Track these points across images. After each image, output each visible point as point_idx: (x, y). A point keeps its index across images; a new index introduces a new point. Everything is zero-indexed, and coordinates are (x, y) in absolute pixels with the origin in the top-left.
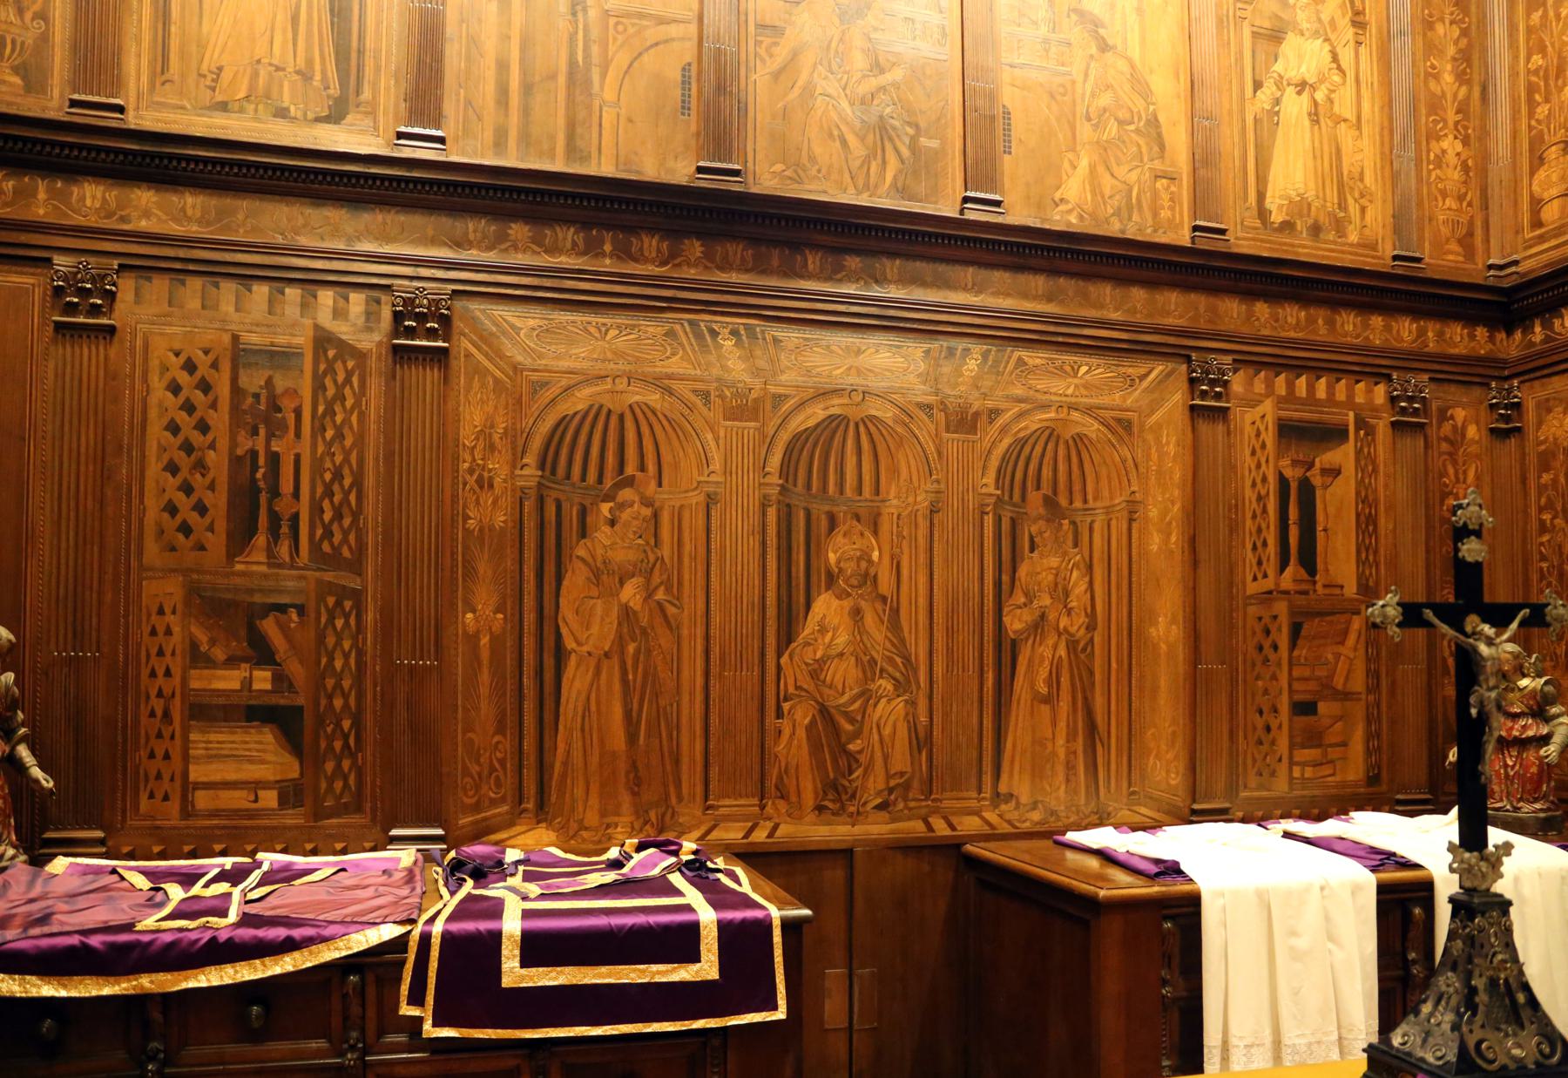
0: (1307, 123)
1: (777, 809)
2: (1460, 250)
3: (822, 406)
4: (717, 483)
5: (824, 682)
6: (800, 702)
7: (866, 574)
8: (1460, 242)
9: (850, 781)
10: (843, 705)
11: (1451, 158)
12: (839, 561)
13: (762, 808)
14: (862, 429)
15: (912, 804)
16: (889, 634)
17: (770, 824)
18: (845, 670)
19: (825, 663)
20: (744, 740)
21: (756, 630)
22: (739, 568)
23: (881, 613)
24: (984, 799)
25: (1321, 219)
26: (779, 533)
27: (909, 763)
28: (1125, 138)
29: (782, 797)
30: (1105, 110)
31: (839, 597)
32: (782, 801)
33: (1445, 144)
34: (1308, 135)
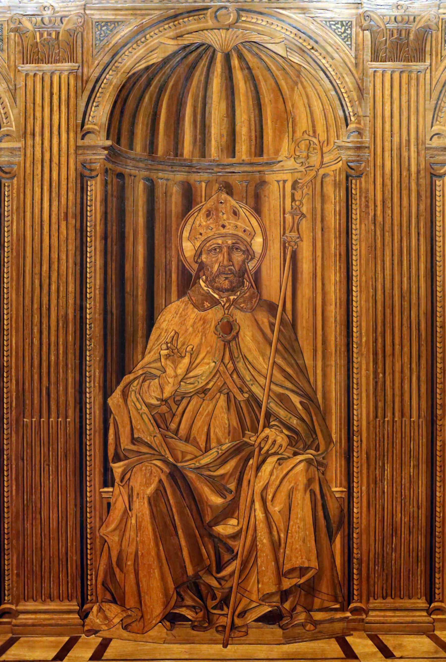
1: (106, 618)
3: (172, 34)
4: (12, 150)
5: (177, 432)
6: (140, 462)
10: (207, 466)
13: (84, 615)
14: (235, 62)
15: (318, 616)
16: (280, 361)
18: (211, 415)
20: (54, 516)
21: (70, 356)
22: (45, 267)
23: (268, 331)
26: (105, 214)
27: (314, 557)
29: (114, 601)
31: (199, 306)
32: (113, 606)
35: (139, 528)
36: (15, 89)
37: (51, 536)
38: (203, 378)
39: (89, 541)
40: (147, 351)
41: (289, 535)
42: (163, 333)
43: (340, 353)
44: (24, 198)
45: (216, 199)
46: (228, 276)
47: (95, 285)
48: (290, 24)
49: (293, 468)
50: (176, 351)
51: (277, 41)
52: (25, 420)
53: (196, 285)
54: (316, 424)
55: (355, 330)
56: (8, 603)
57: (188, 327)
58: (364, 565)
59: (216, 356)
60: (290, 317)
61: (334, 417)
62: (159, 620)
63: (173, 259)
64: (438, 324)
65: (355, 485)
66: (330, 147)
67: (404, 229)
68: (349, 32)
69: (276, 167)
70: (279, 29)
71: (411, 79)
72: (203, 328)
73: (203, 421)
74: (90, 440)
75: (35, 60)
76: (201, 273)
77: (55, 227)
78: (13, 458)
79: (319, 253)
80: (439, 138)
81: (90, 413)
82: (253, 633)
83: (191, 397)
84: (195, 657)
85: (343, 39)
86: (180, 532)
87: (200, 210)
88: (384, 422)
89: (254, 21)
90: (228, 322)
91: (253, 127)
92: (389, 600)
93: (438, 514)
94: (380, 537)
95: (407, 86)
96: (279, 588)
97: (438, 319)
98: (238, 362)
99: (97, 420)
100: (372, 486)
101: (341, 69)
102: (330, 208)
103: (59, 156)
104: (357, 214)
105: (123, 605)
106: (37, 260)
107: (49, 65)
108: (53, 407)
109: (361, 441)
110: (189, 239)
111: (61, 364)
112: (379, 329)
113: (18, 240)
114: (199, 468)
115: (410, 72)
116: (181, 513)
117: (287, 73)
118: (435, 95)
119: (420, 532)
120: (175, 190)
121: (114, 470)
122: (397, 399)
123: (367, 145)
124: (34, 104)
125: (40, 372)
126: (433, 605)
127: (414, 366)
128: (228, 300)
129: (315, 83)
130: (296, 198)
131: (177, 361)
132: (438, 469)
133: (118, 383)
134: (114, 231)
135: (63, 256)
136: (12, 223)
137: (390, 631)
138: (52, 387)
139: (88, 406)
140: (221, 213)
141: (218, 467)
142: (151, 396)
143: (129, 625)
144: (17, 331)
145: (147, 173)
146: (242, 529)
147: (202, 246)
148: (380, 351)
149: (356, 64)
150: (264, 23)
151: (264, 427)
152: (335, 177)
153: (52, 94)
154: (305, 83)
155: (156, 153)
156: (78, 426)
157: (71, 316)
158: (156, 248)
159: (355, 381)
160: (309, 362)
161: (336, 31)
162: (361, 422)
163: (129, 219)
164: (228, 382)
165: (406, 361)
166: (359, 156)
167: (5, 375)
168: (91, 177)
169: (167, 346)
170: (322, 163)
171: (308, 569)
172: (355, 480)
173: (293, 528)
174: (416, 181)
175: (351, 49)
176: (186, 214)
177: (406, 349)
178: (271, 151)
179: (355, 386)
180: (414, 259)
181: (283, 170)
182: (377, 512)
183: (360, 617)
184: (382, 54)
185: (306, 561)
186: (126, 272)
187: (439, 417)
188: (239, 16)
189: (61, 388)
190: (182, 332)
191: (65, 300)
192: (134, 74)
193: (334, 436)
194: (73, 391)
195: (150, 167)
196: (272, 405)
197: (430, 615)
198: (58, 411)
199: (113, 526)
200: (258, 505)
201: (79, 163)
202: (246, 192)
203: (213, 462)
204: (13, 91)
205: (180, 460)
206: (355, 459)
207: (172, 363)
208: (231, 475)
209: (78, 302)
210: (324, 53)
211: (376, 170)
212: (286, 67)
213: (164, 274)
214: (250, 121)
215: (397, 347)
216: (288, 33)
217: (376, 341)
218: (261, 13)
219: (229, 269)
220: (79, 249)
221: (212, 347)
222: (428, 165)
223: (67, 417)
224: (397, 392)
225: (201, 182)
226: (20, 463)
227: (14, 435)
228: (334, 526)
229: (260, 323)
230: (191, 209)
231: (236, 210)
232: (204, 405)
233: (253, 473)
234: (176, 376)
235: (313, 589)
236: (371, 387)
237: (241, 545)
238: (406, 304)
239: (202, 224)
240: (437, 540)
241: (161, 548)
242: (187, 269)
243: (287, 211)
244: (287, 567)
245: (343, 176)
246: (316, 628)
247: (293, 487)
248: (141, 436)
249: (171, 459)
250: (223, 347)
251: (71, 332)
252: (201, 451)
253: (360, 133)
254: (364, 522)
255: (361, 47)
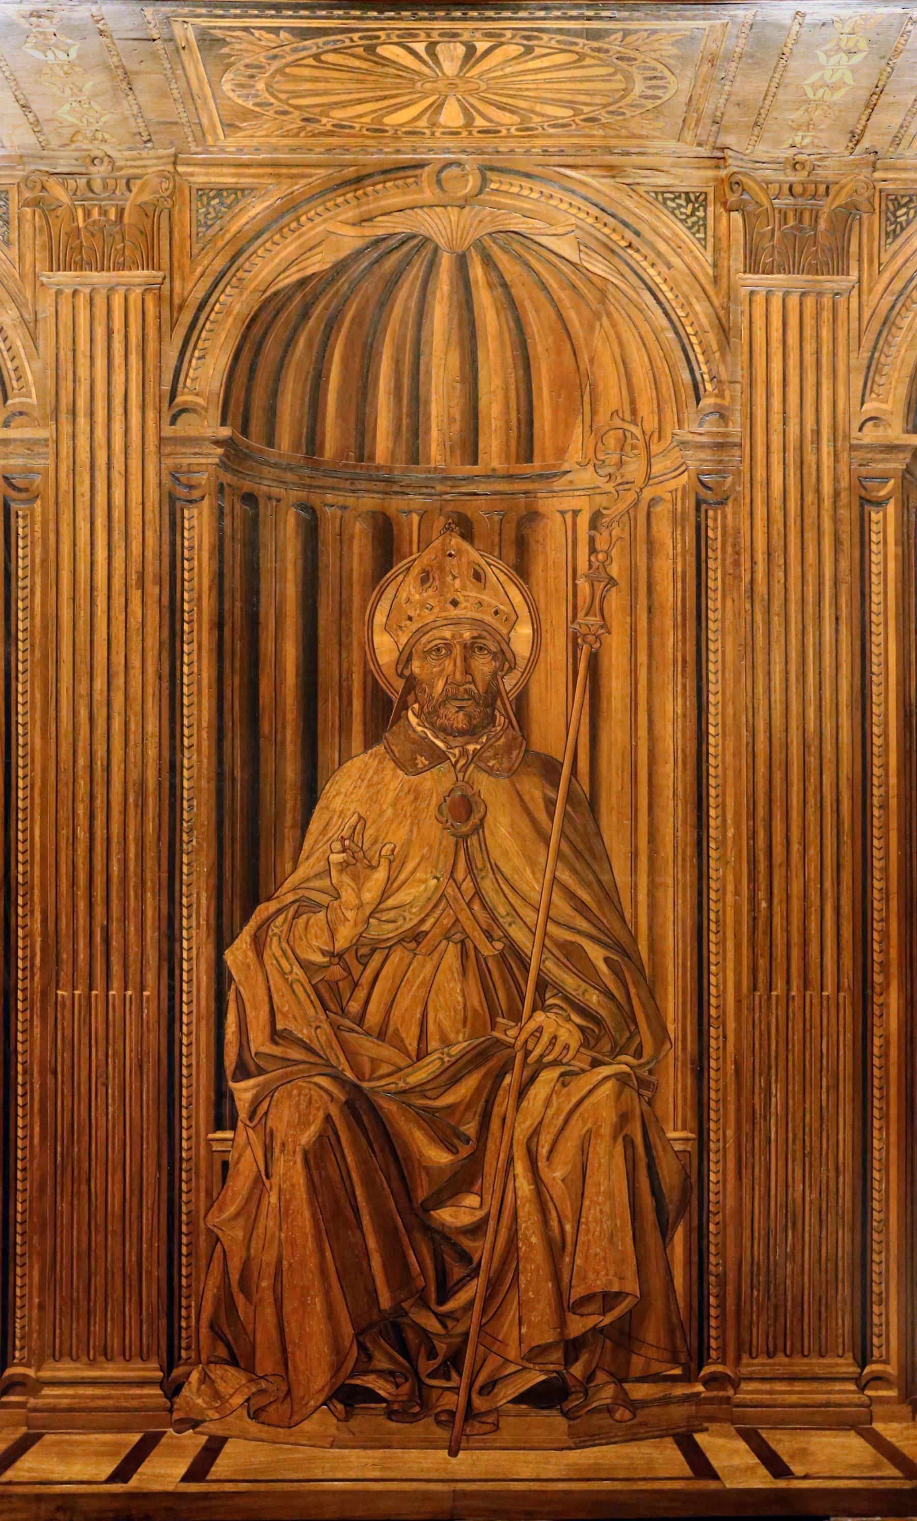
1: (217, 1395)
4: (30, 444)
5: (361, 1019)
7: (492, 695)
9: (442, 1318)
10: (421, 1089)
12: (405, 658)
13: (173, 1390)
14: (477, 272)
15: (640, 1391)
16: (565, 876)
17: (194, 1441)
18: (429, 985)
19: (363, 962)
20: (115, 1189)
21: (150, 863)
22: (100, 683)
24: (879, 1379)
27: (630, 1270)
29: (233, 1361)
31: (406, 765)
32: (231, 1371)
35: (284, 1213)
36: (36, 321)
37: (110, 1228)
38: (414, 910)
39: (184, 1240)
40: (303, 854)
41: (583, 1227)
42: (336, 817)
43: (683, 860)
44: (57, 542)
45: (440, 546)
46: (464, 704)
47: (199, 721)
48: (585, 199)
49: (590, 1092)
50: (361, 855)
51: (561, 230)
52: (60, 992)
53: (402, 722)
54: (635, 1002)
55: (712, 812)
56: (21, 1364)
57: (384, 807)
58: (730, 1289)
59: (440, 866)
60: (586, 788)
61: (671, 989)
62: (321, 1399)
63: (355, 669)
64: (876, 801)
65: (712, 1125)
66: (665, 444)
67: (810, 609)
68: (701, 213)
69: (559, 484)
70: (564, 206)
71: (822, 309)
72: (415, 809)
73: (414, 997)
74: (189, 1034)
75: (76, 263)
76: (410, 698)
77: (118, 601)
78: (36, 1069)
79: (643, 658)
80: (875, 425)
81: (190, 981)
82: (510, 1427)
83: (390, 947)
84: (393, 1475)
85: (689, 228)
86: (366, 1220)
87: (408, 569)
88: (769, 998)
89: (515, 190)
90: (463, 797)
91: (513, 403)
92: (781, 1358)
93: (876, 1185)
94: (762, 1232)
95: (813, 322)
96: (561, 1334)
97: (876, 791)
98: (482, 878)
99: (203, 994)
100: (746, 1128)
101: (685, 288)
102: (665, 566)
103: (126, 458)
104: (716, 579)
105: (250, 1369)
106: (83, 668)
107: (104, 274)
108: (116, 968)
109: (725, 1037)
110: (386, 628)
111: (132, 881)
112: (761, 812)
113: (45, 627)
114: (404, 1092)
115: (820, 294)
116: (369, 1182)
117: (582, 297)
118: (868, 340)
119: (840, 1221)
120: (359, 528)
121: (236, 1095)
122: (795, 953)
123: (737, 440)
124: (74, 351)
125: (91, 896)
126: (867, 1369)
127: (828, 884)
128: (464, 753)
129: (635, 313)
130: (598, 547)
131: (362, 876)
132: (876, 1093)
133: (245, 919)
134: (237, 611)
135: (136, 662)
136: (33, 592)
137: (783, 1422)
138: (114, 926)
139: (185, 966)
140: (451, 577)
141: (442, 1090)
142: (311, 946)
143: (262, 1409)
144: (44, 812)
145: (301, 494)
146: (488, 1215)
147: (412, 641)
148: (761, 857)
149: (715, 277)
150: (535, 195)
151: (534, 1010)
152: (674, 504)
153: (110, 332)
154: (616, 315)
155: (321, 452)
156: (165, 1005)
157: (151, 784)
158: (321, 646)
159: (713, 916)
160: (622, 877)
161: (677, 212)
162: (725, 1000)
163: (266, 587)
164: (463, 918)
165: (812, 876)
166: (721, 461)
167: (20, 901)
168: (191, 502)
169: (343, 845)
170: (648, 477)
171: (620, 1295)
172: (713, 1115)
173: (591, 1213)
174: (831, 511)
175: (705, 247)
176: (381, 578)
177: (813, 852)
178: (550, 452)
179: (713, 927)
180: (828, 670)
181: (572, 490)
182: (756, 1181)
183: (722, 1393)
184: (765, 259)
185: (616, 1280)
186: (261, 694)
187: (877, 989)
188: (485, 181)
189: (132, 928)
190: (373, 816)
191: (139, 749)
192: (276, 294)
193: (671, 1027)
194: (156, 934)
195: (308, 481)
196: (549, 964)
197: (862, 1389)
198: (126, 975)
199: (232, 1210)
200: (520, 1168)
201: (165, 473)
202: (500, 534)
203: (433, 1079)
204: (32, 325)
205: (367, 1076)
206: (713, 1074)
207: (353, 879)
208: (468, 1107)
209: (166, 754)
210: (652, 256)
211: (754, 490)
212: (579, 284)
213: (337, 698)
214: (507, 390)
215: (796, 847)
216: (582, 215)
217: (753, 836)
218: (528, 176)
219: (465, 690)
220: (167, 646)
221: (431, 848)
222: (855, 482)
223: (142, 989)
224: (796, 938)
225: (410, 512)
226: (50, 1079)
227: (36, 1022)
228: (671, 1208)
229: (526, 798)
230: (392, 568)
231: (480, 571)
232: (415, 964)
233: (512, 1102)
234: (360, 906)
235: (629, 1336)
236: (745, 928)
237: (488, 1246)
238: (813, 761)
239: (412, 598)
240: (876, 1236)
241: (328, 1254)
242: (382, 689)
243: (579, 573)
244: (578, 1292)
245: (691, 503)
246: (635, 1416)
247: (589, 1131)
248: (291, 1026)
249: (349, 1074)
250: (452, 847)
251: (151, 815)
252: (410, 1057)
253: (722, 415)
254: (730, 1202)
255: (724, 244)
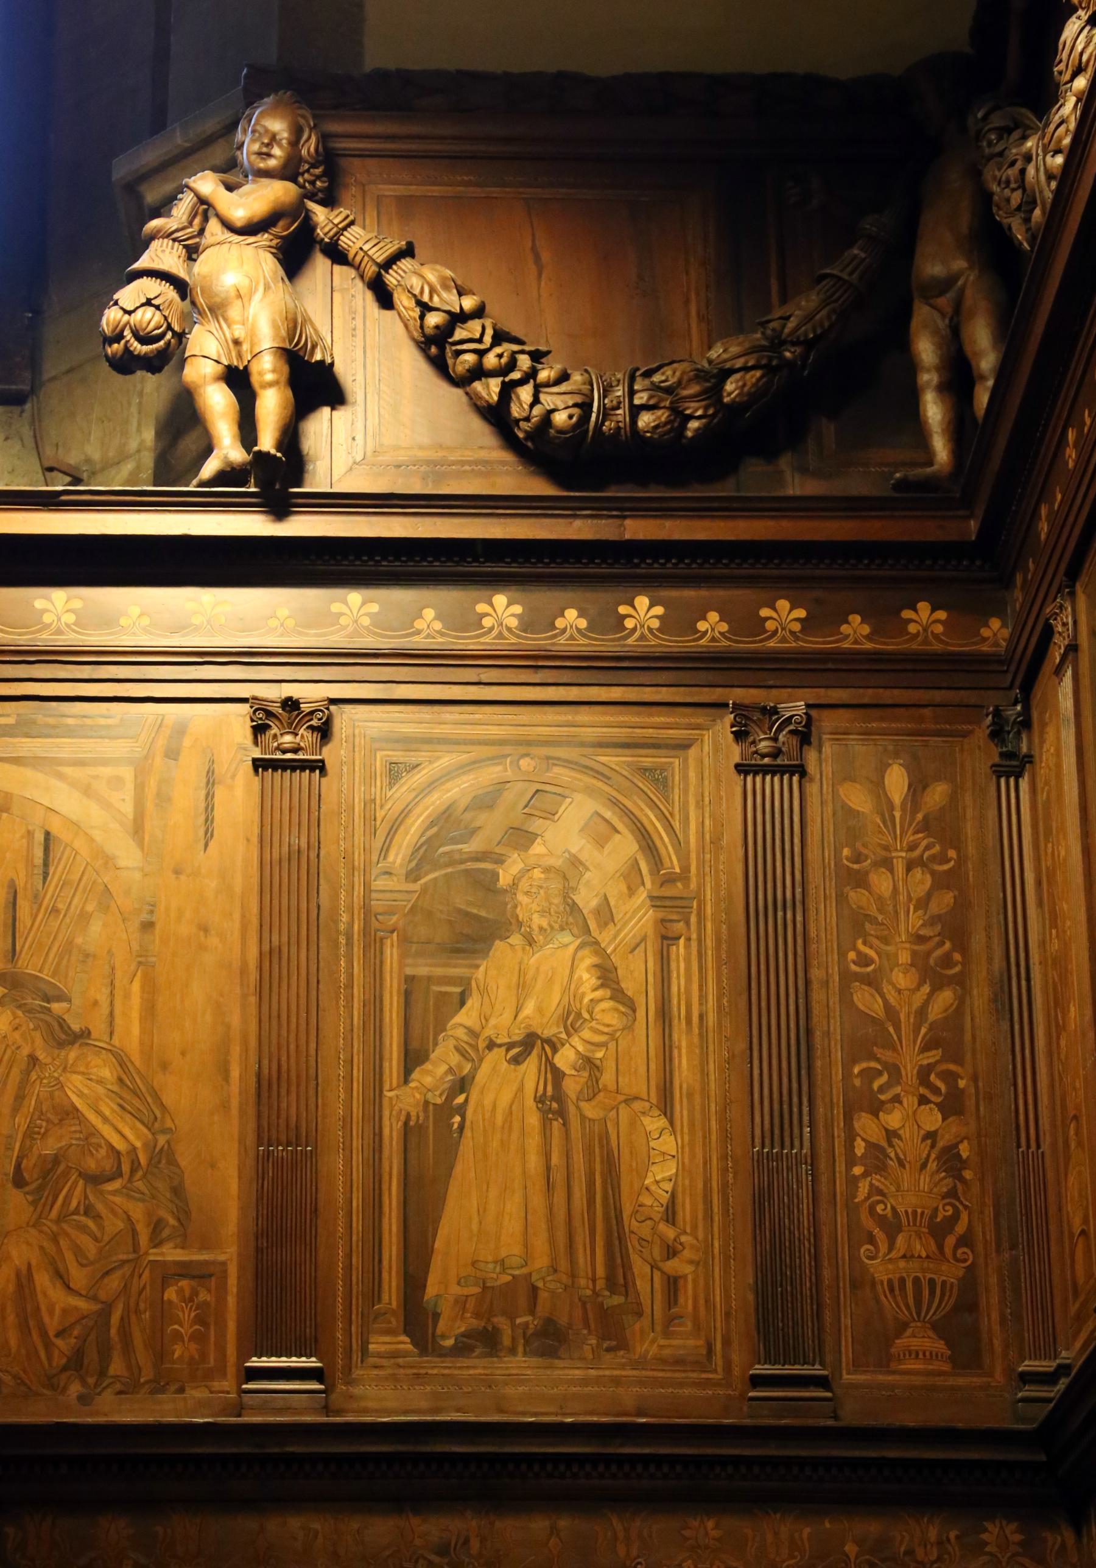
0: (533, 1120)
2: (940, 1346)
8: (939, 1328)
11: (911, 1146)
25: (563, 1321)
28: (100, 1207)
30: (56, 1160)
33: (893, 1119)
34: (534, 1142)
